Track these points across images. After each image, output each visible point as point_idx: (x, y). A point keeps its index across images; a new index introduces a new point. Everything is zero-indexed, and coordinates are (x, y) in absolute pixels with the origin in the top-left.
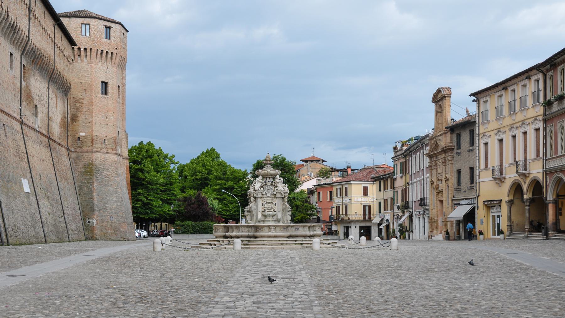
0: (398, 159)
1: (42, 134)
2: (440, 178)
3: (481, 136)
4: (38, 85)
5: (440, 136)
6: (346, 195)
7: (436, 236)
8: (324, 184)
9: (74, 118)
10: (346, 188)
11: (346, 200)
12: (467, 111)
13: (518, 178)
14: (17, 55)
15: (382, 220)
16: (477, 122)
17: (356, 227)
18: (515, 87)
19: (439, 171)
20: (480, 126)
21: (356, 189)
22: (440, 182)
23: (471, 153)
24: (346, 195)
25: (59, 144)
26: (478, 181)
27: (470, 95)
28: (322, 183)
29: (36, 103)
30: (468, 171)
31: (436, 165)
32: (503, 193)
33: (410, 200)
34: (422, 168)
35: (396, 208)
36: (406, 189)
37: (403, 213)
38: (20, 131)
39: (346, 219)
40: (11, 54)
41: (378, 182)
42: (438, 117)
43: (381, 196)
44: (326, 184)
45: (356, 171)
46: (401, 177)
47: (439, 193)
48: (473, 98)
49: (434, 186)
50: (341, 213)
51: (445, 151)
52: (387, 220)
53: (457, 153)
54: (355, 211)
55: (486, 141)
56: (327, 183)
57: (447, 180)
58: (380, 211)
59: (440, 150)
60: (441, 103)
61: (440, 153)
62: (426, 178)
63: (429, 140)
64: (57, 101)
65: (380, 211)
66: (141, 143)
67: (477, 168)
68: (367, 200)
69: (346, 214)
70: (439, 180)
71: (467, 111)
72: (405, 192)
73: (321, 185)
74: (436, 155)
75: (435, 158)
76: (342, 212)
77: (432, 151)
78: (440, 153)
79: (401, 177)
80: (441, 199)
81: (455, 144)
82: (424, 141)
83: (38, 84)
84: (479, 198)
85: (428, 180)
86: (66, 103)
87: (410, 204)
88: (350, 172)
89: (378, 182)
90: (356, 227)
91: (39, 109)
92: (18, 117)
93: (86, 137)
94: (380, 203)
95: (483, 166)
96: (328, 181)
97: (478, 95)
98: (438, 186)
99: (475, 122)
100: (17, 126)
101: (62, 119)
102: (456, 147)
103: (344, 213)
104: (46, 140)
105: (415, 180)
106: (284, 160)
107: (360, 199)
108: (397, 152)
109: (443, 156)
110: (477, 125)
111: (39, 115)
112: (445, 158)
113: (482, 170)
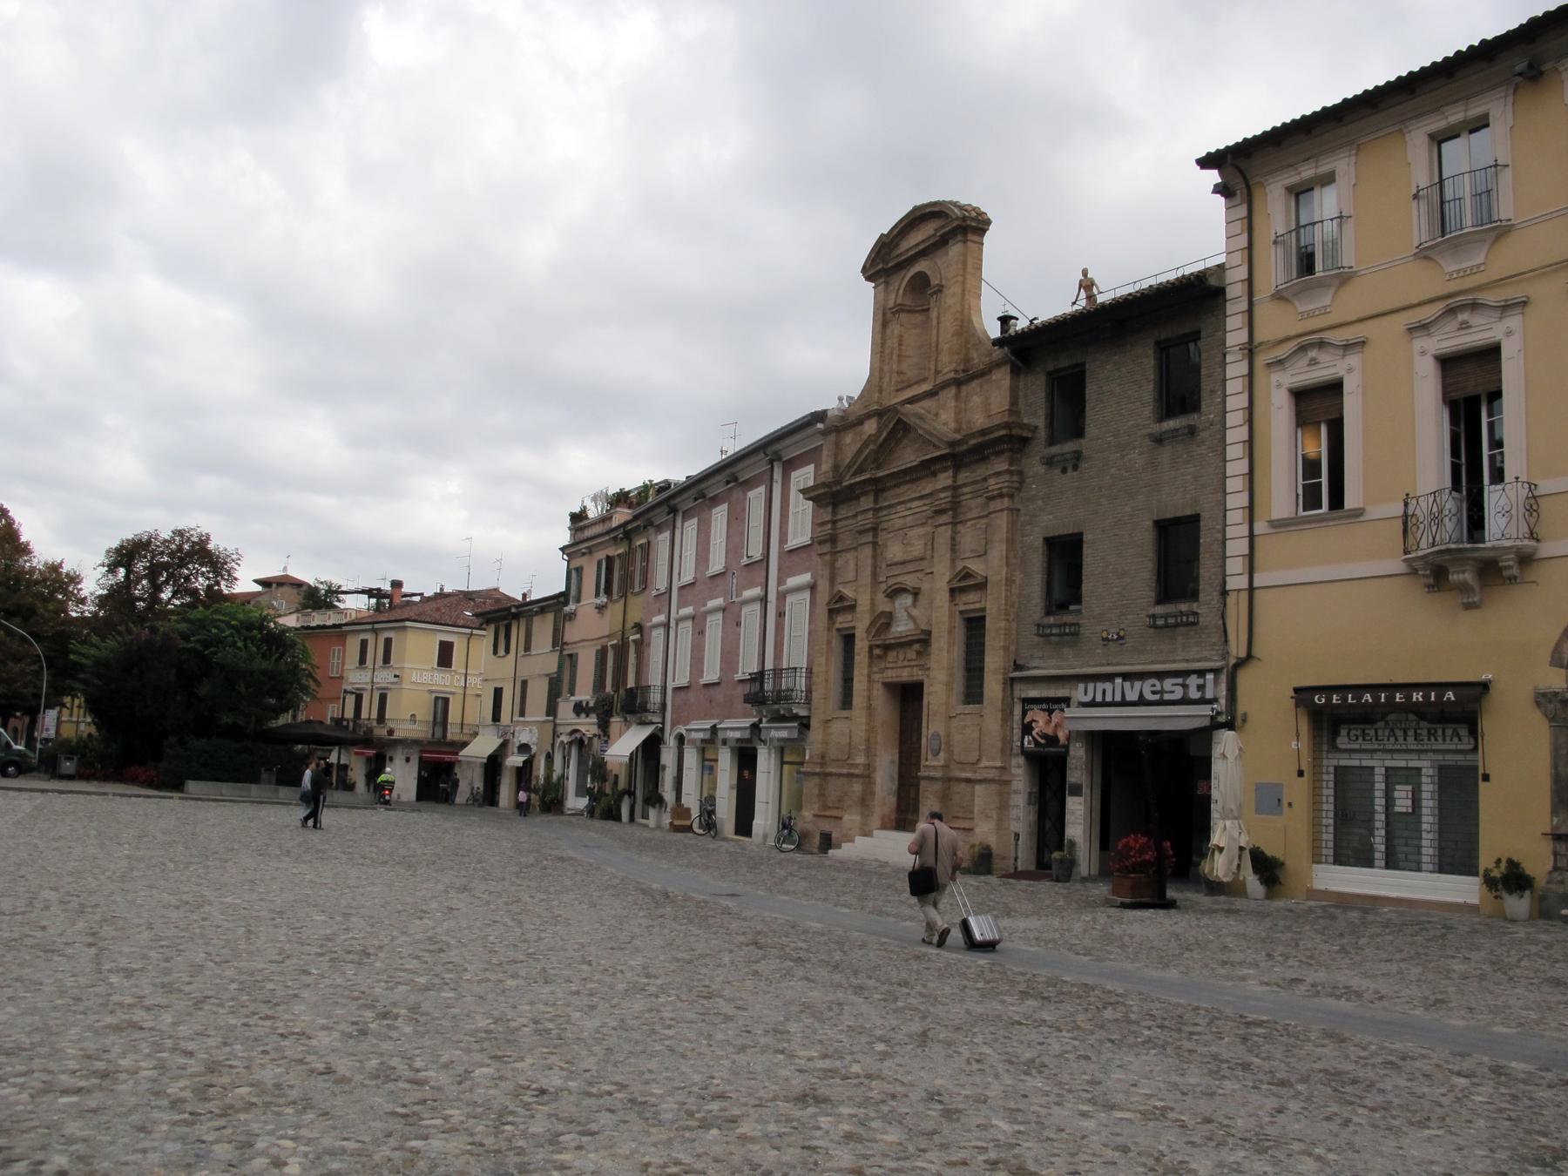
0: (590, 551)
2: (910, 581)
3: (1261, 360)
5: (911, 401)
6: (387, 659)
7: (859, 840)
8: (319, 627)
10: (388, 642)
11: (384, 677)
12: (1087, 285)
15: (504, 746)
16: (1235, 291)
17: (408, 760)
19: (895, 551)
20: (1263, 312)
21: (417, 647)
23: (1165, 454)
24: (387, 659)
26: (1237, 582)
27: (1206, 162)
28: (313, 624)
30: (1146, 537)
33: (654, 678)
34: (756, 552)
35: (565, 710)
36: (621, 651)
37: (604, 726)
39: (381, 732)
41: (492, 628)
42: (895, 329)
43: (504, 670)
44: (324, 627)
45: (417, 599)
46: (601, 608)
47: (887, 648)
48: (1214, 176)
50: (364, 715)
51: (965, 454)
52: (524, 748)
53: (1049, 462)
54: (408, 716)
56: (329, 623)
58: (496, 717)
59: (908, 456)
61: (928, 468)
62: (782, 597)
63: (824, 433)
65: (496, 717)
67: (1235, 517)
68: (445, 681)
69: (381, 718)
70: (894, 593)
71: (1087, 285)
72: (622, 652)
73: (308, 628)
74: (878, 487)
75: (867, 502)
76: (369, 711)
77: (860, 471)
78: (928, 468)
79: (601, 608)
80: (905, 675)
81: (1036, 418)
82: (777, 447)
84: (1245, 678)
87: (655, 697)
88: (397, 600)
89: (492, 628)
90: (408, 760)
94: (498, 693)
97: (1239, 167)
98: (884, 621)
99: (1220, 292)
102: (1042, 434)
103: (374, 715)
105: (688, 610)
107: (426, 678)
108: (582, 529)
109: (944, 479)
112: (955, 488)
113: (1277, 525)
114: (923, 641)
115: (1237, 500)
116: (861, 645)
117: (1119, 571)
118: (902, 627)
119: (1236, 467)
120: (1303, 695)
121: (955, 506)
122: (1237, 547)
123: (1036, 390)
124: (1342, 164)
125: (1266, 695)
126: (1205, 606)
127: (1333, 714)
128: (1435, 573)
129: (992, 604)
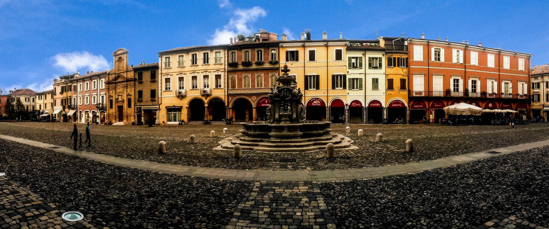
13: (201, 97)
16: (160, 67)
18: (197, 53)
32: (185, 104)
57: (128, 95)
95: (164, 89)
114: (123, 101)
115: (160, 89)
117: (147, 95)
118: (120, 99)
119: (160, 85)
120: (166, 107)
121: (127, 86)
122: (160, 93)
123: (137, 74)
124: (171, 56)
125: (163, 107)
126: (156, 99)
127: (170, 109)
128: (178, 97)
129: (132, 98)
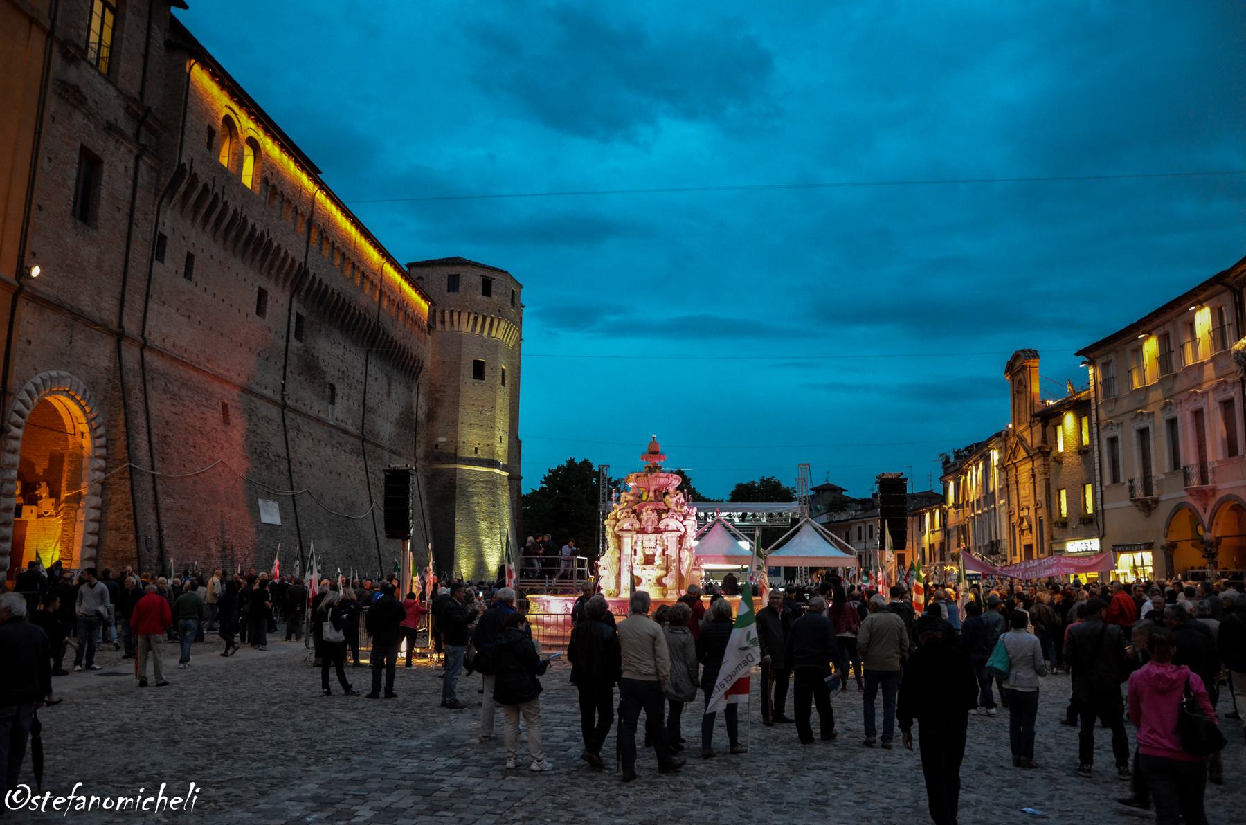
1: (345, 432)
4: (334, 352)
9: (431, 416)
14: (279, 299)
16: (1093, 401)
19: (1023, 493)
22: (1026, 512)
25: (392, 452)
27: (1077, 354)
29: (329, 379)
31: (1017, 482)
38: (279, 421)
40: (262, 294)
49: (1015, 519)
55: (1112, 434)
60: (1021, 376)
64: (389, 385)
66: (571, 462)
83: (339, 352)
85: (1004, 509)
86: (415, 390)
91: (338, 391)
92: (280, 401)
93: (447, 444)
96: (844, 516)
98: (1022, 519)
99: (1089, 401)
100: (274, 413)
101: (401, 414)
104: (359, 443)
106: (778, 484)
110: (1093, 407)
111: (338, 400)
116: (1017, 530)
